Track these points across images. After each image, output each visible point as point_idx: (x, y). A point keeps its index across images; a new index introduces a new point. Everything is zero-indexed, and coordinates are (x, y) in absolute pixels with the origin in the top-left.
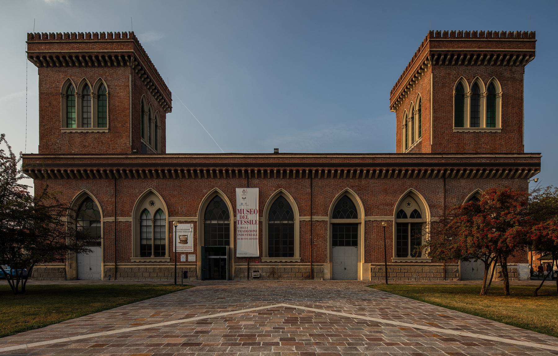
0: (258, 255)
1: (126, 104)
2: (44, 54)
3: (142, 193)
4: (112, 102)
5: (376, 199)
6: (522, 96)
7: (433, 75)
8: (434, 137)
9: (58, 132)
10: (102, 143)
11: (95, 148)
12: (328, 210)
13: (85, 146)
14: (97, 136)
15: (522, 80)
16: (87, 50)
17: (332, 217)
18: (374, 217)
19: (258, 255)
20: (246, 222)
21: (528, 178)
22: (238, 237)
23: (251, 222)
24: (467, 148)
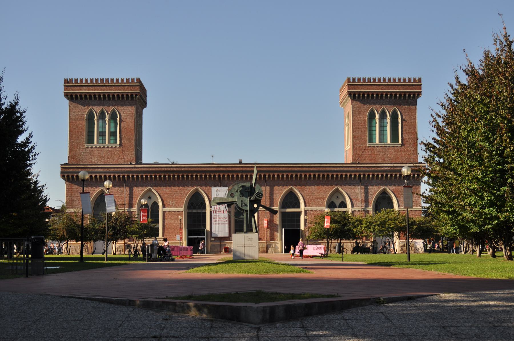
0: (228, 236)
1: (132, 126)
2: (76, 94)
3: (143, 191)
4: (122, 124)
5: (312, 194)
6: (416, 121)
7: (352, 106)
8: (354, 150)
9: (83, 147)
10: (114, 154)
11: (109, 158)
12: (278, 203)
13: (102, 157)
14: (110, 149)
15: (416, 109)
16: (107, 91)
17: (281, 207)
18: (311, 207)
19: (228, 236)
20: (218, 212)
21: (420, 178)
22: (213, 223)
23: (222, 212)
24: (377, 157)
